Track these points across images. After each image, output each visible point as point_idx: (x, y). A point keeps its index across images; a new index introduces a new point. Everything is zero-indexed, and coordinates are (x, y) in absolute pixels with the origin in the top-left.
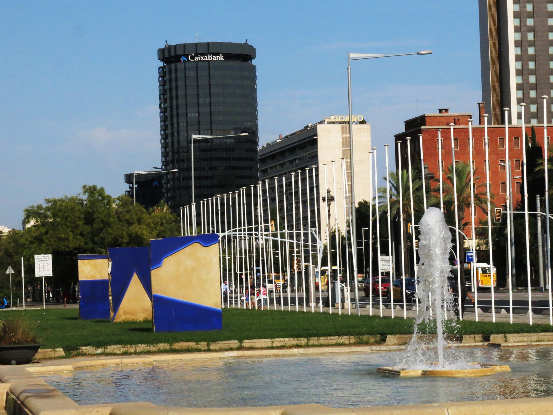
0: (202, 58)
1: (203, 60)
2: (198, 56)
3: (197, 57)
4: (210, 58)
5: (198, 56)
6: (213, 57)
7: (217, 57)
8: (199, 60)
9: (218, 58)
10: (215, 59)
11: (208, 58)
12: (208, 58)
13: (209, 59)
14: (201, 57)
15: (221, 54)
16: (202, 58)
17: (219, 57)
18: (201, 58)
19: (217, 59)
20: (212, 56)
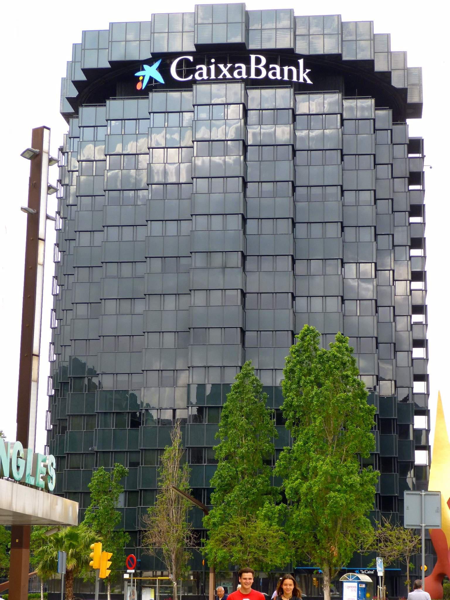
0: (225, 71)
1: (229, 76)
2: (209, 64)
3: (204, 67)
4: (258, 72)
5: (209, 64)
6: (268, 69)
7: (286, 69)
8: (213, 76)
9: (290, 72)
10: (279, 77)
11: (248, 72)
12: (248, 72)
13: (253, 76)
14: (221, 66)
15: (301, 62)
16: (225, 71)
17: (294, 69)
18: (218, 71)
19: (286, 78)
20: (264, 60)
